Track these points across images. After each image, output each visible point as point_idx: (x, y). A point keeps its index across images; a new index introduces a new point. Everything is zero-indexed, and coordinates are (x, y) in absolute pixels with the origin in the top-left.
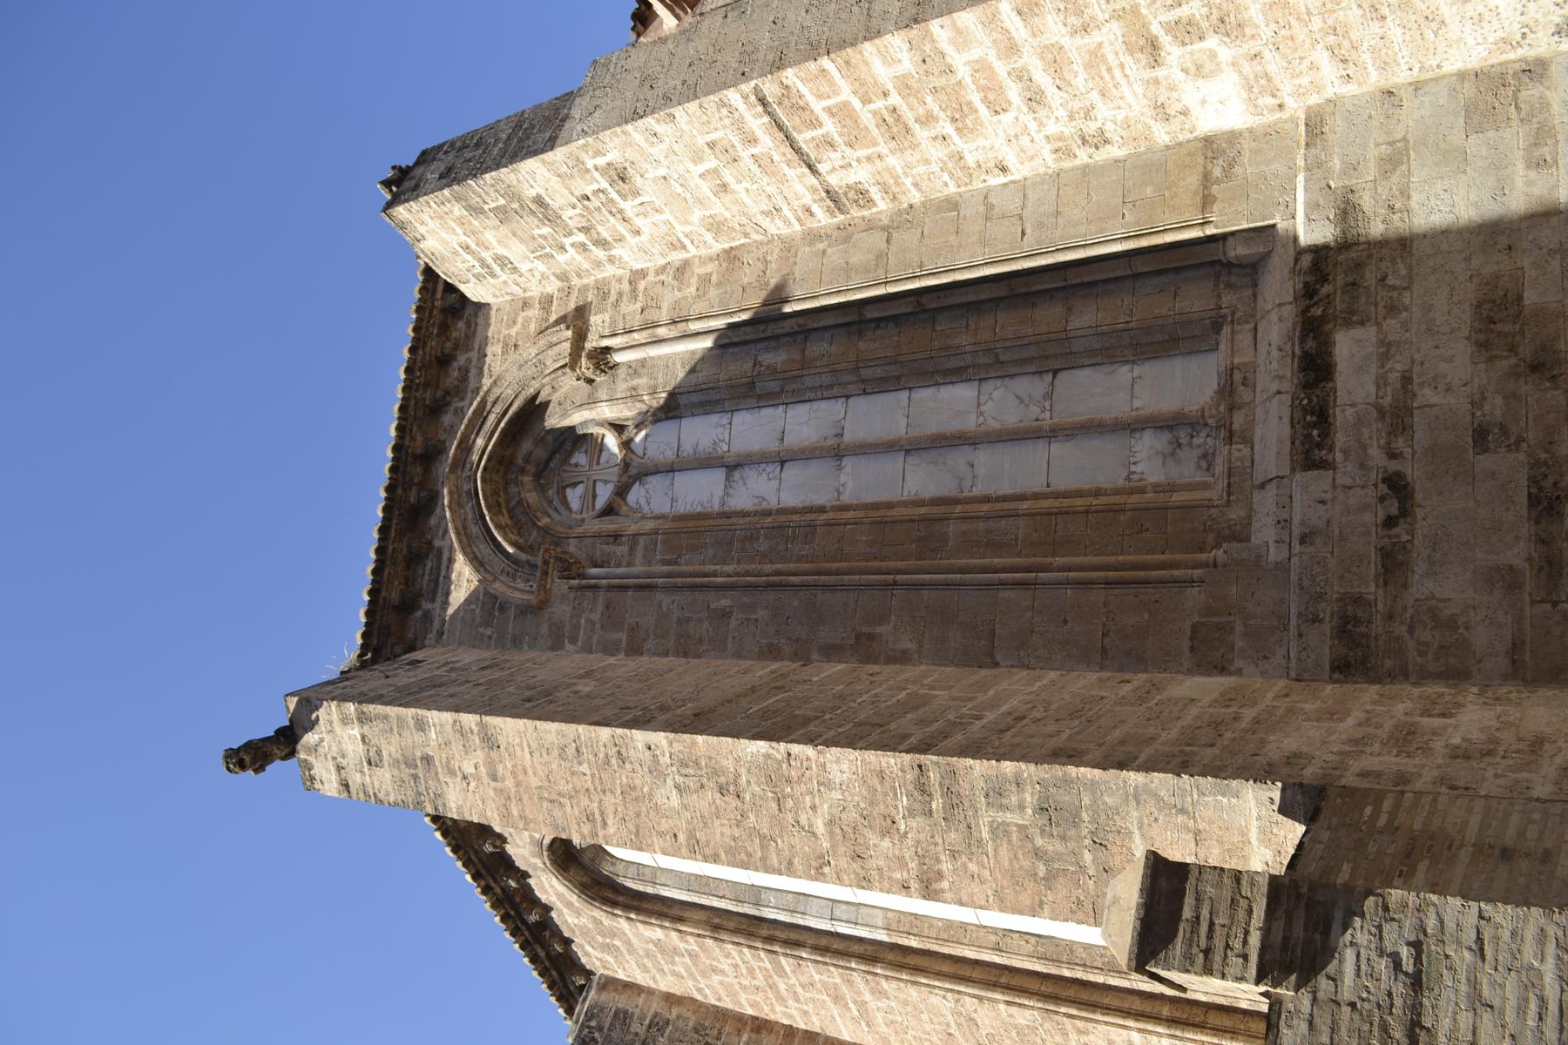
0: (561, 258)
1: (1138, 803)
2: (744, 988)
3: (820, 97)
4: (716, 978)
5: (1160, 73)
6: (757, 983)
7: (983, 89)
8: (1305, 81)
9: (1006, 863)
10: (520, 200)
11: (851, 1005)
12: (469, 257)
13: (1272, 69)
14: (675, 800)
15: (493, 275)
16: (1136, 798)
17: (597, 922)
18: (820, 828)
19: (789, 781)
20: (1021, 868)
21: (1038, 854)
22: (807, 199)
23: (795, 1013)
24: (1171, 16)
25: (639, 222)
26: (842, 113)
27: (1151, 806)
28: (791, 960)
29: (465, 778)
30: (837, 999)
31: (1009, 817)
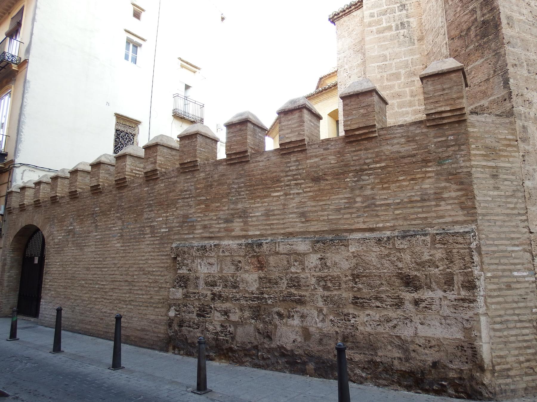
1: (494, 56)
9: (463, 20)
16: (496, 54)
20: (463, 26)
27: (494, 60)
31: (479, 12)
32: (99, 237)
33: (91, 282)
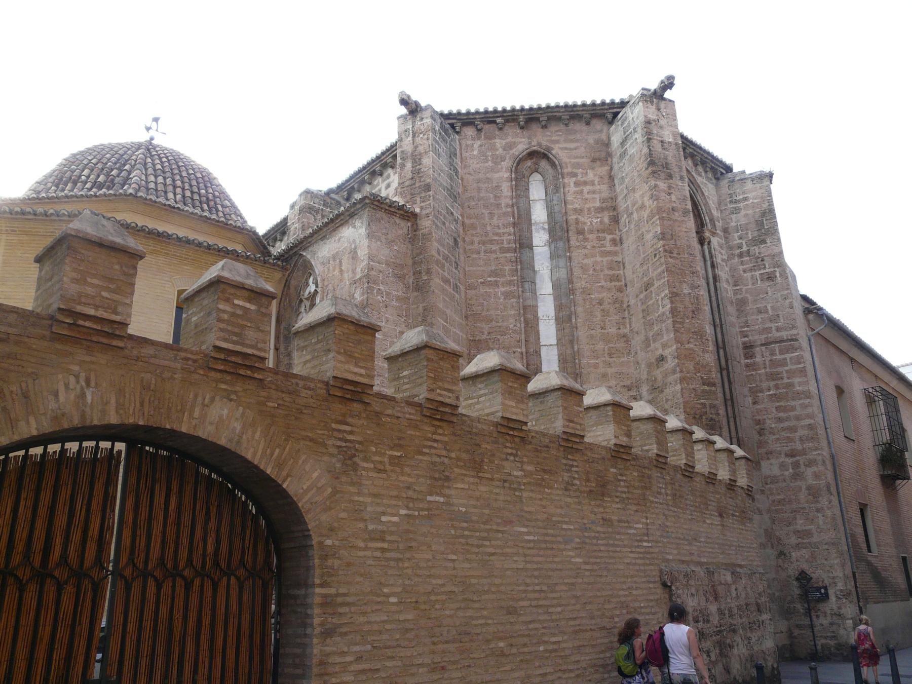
0: (736, 235)
2: (485, 225)
3: (791, 358)
4: (486, 212)
5: (783, 456)
6: (490, 234)
7: (785, 407)
8: (774, 491)
10: (765, 234)
11: (492, 279)
12: (741, 197)
13: (780, 484)
14: (686, 292)
15: (731, 202)
17: (503, 159)
18: (692, 346)
19: (701, 338)
21: (701, 416)
22: (751, 338)
23: (476, 246)
24: (801, 463)
25: (749, 275)
26: (783, 363)
28: (514, 259)
29: (669, 194)
30: (494, 273)
31: (708, 409)
32: (531, 538)
33: (526, 640)
